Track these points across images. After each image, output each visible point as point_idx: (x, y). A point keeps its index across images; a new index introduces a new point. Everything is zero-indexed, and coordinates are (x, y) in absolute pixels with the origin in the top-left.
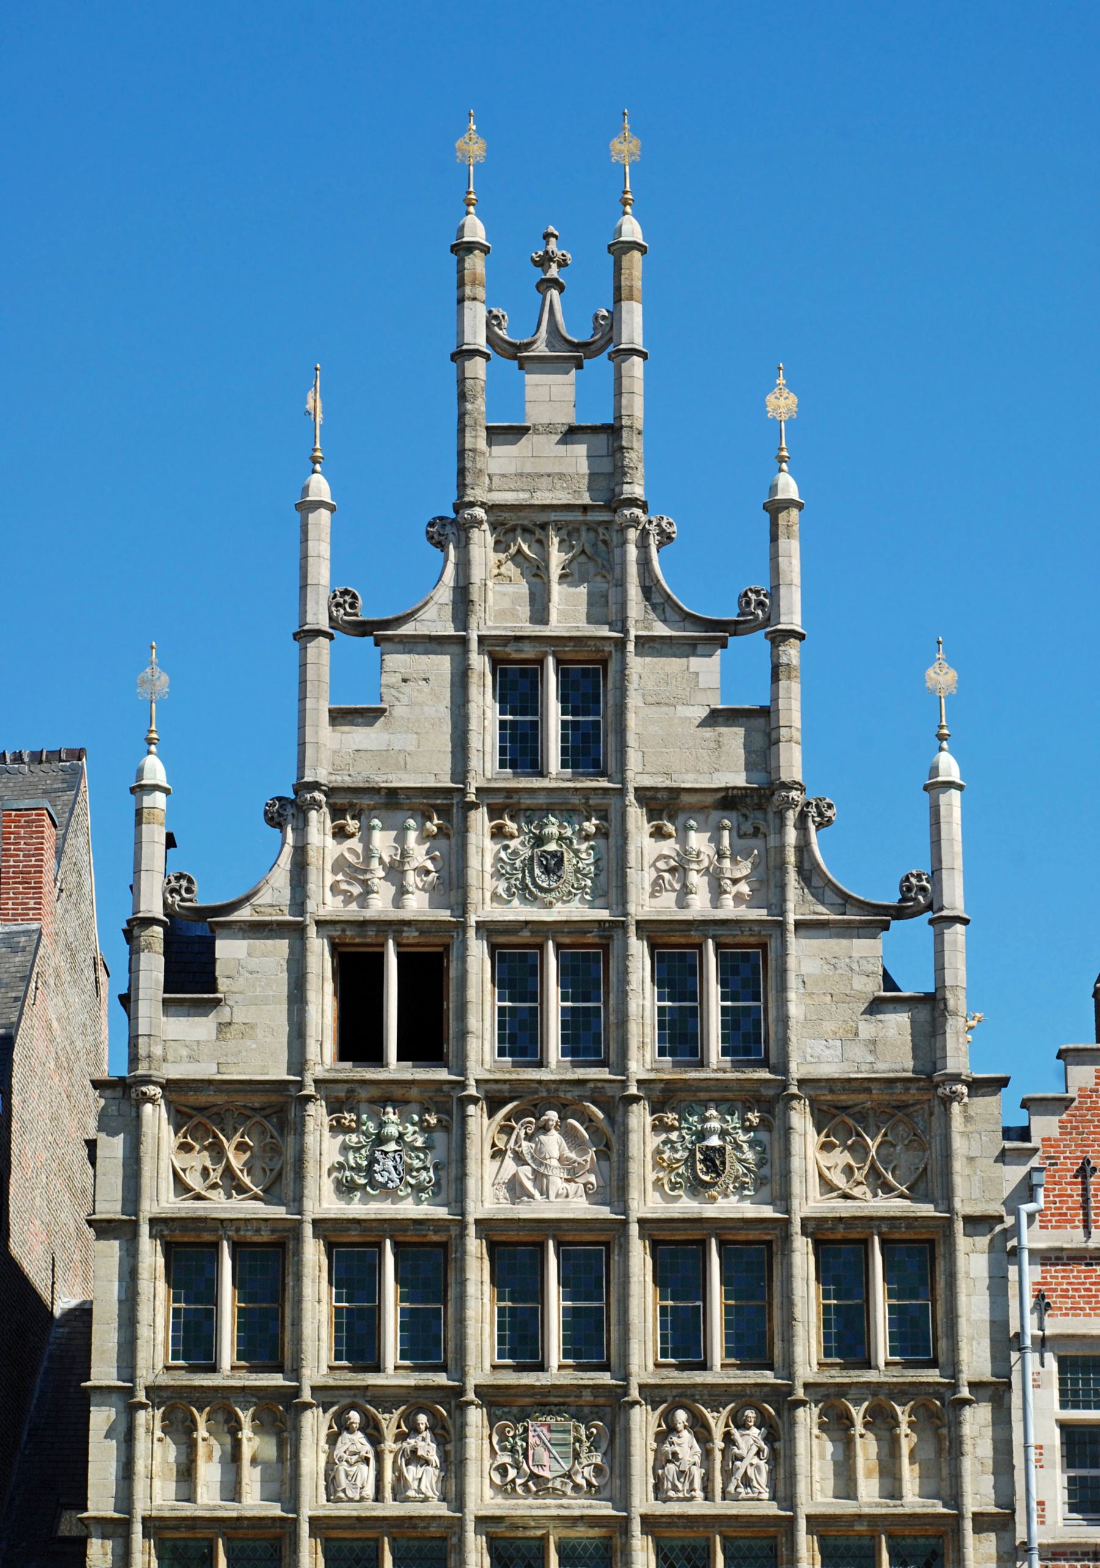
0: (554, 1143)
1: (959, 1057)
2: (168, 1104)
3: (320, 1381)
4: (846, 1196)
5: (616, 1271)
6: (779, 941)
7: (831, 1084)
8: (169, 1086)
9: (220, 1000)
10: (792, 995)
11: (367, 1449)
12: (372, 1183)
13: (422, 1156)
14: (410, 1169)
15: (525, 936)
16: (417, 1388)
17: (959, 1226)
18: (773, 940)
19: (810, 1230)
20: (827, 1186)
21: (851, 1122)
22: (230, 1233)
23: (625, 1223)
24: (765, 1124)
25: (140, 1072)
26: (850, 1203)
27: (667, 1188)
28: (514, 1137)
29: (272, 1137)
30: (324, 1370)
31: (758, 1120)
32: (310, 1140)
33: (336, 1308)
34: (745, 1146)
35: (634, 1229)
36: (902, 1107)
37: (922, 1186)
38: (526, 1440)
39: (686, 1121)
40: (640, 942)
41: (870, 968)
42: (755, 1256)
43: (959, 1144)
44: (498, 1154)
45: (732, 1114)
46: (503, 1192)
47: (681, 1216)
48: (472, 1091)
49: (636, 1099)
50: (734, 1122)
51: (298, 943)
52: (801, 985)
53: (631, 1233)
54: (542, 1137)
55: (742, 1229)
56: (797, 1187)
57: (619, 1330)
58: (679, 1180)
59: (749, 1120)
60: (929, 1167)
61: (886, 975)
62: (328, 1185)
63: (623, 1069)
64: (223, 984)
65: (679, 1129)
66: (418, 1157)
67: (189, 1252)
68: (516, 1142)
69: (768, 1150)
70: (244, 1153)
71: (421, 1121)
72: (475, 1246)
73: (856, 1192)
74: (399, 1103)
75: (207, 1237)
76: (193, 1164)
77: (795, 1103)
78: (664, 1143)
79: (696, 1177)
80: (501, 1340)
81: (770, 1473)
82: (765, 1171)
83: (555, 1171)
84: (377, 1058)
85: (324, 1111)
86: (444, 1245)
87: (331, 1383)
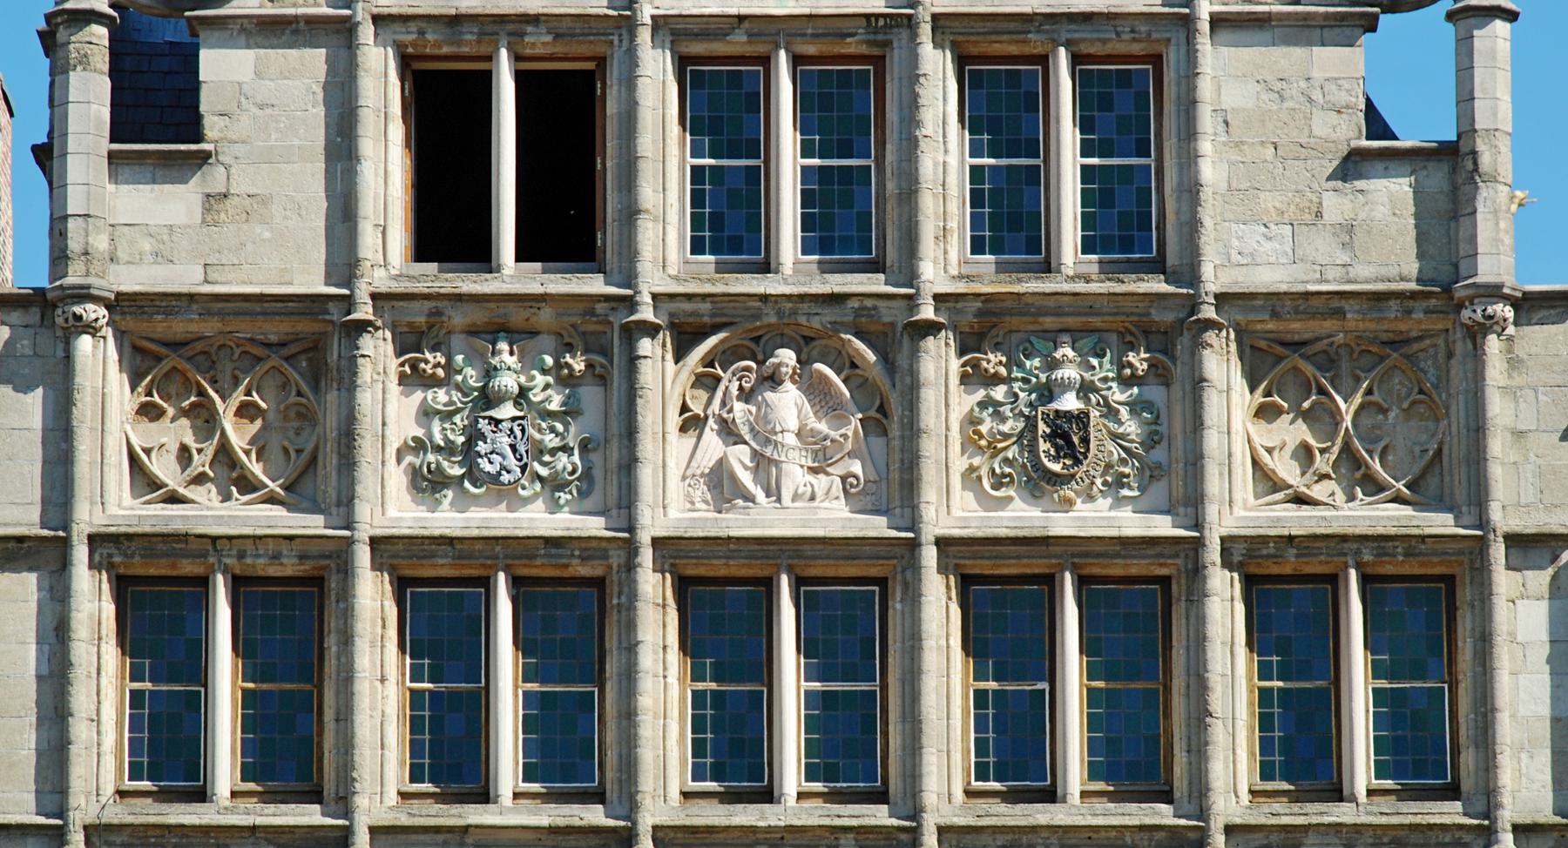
0: (789, 405)
1: (1498, 257)
2: (120, 336)
3: (386, 819)
4: (1300, 500)
5: (899, 628)
6: (1183, 50)
7: (1273, 301)
8: (120, 304)
9: (204, 157)
10: (1205, 146)
12: (473, 474)
13: (560, 427)
14: (539, 451)
15: (738, 43)
16: (553, 830)
17: (1498, 551)
18: (1172, 49)
19: (1236, 558)
20: (1267, 481)
21: (1309, 369)
22: (228, 561)
23: (914, 545)
24: (1159, 373)
25: (70, 280)
26: (1306, 511)
27: (986, 484)
28: (719, 394)
29: (299, 394)
30: (392, 798)
31: (1145, 366)
32: (366, 399)
33: (412, 691)
34: (1124, 412)
35: (930, 555)
36: (1398, 342)
37: (1432, 482)
39: (1021, 366)
40: (939, 52)
41: (1342, 98)
42: (1140, 604)
43: (1498, 408)
44: (692, 424)
45: (1101, 356)
46: (701, 491)
47: (1012, 533)
48: (646, 313)
49: (932, 328)
50: (1104, 368)
51: (343, 53)
52: (1221, 128)
53: (924, 563)
54: (769, 395)
55: (1118, 556)
56: (1214, 484)
58: (1008, 470)
59: (1130, 365)
60: (1445, 451)
61: (1371, 110)
62: (397, 478)
63: (910, 276)
64: (212, 126)
65: (1008, 380)
66: (552, 430)
67: (158, 592)
68: (723, 404)
69: (1164, 419)
70: (252, 421)
71: (559, 366)
72: (652, 585)
73: (1319, 491)
74: (519, 335)
75: (188, 568)
76: (163, 440)
77: (1210, 336)
78: (982, 405)
79: (1038, 466)
80: (698, 748)
82: (1159, 454)
83: (791, 454)
84: (480, 254)
85: (390, 348)
86: (599, 583)
87: (405, 820)
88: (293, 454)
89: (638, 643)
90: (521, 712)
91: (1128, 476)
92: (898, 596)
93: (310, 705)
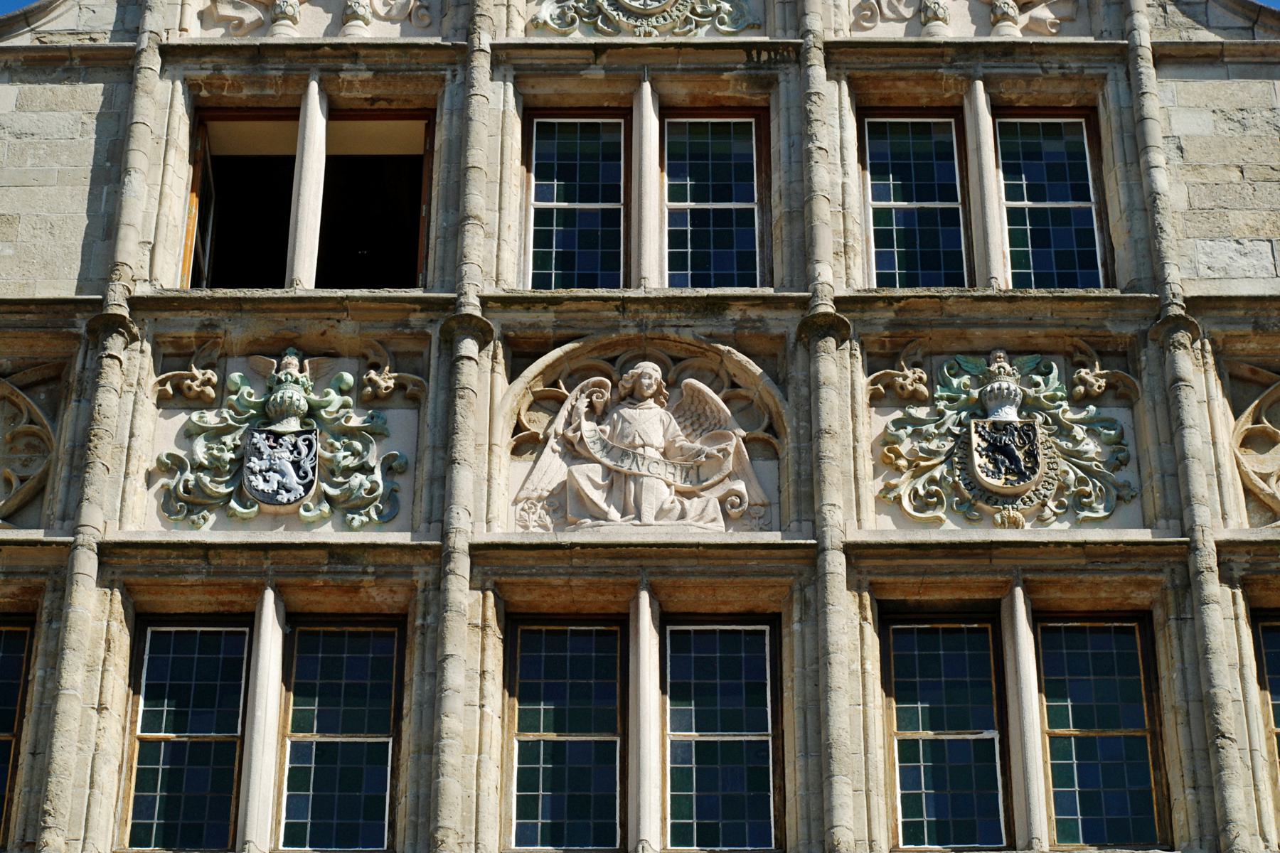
5: (797, 651)
6: (1123, 85)
10: (1157, 157)
13: (358, 445)
14: (330, 471)
18: (1110, 89)
19: (1237, 573)
23: (815, 554)
24: (1119, 393)
28: (564, 413)
29: (31, 422)
31: (1103, 382)
33: (141, 740)
34: (1079, 432)
35: (836, 564)
39: (946, 385)
40: (833, 86)
44: (526, 444)
45: (1046, 373)
50: (1052, 384)
51: (123, 88)
52: (1175, 154)
53: (829, 568)
54: (626, 412)
55: (1083, 571)
57: (806, 769)
58: (934, 488)
59: (1083, 381)
65: (930, 401)
66: (347, 448)
68: (568, 423)
69: (1129, 438)
71: (360, 385)
72: (468, 607)
78: (899, 424)
79: (972, 482)
80: (526, 807)
85: (148, 361)
86: (399, 620)
88: (15, 483)
89: (446, 657)
90: (287, 765)
91: (1089, 495)
92: (796, 615)
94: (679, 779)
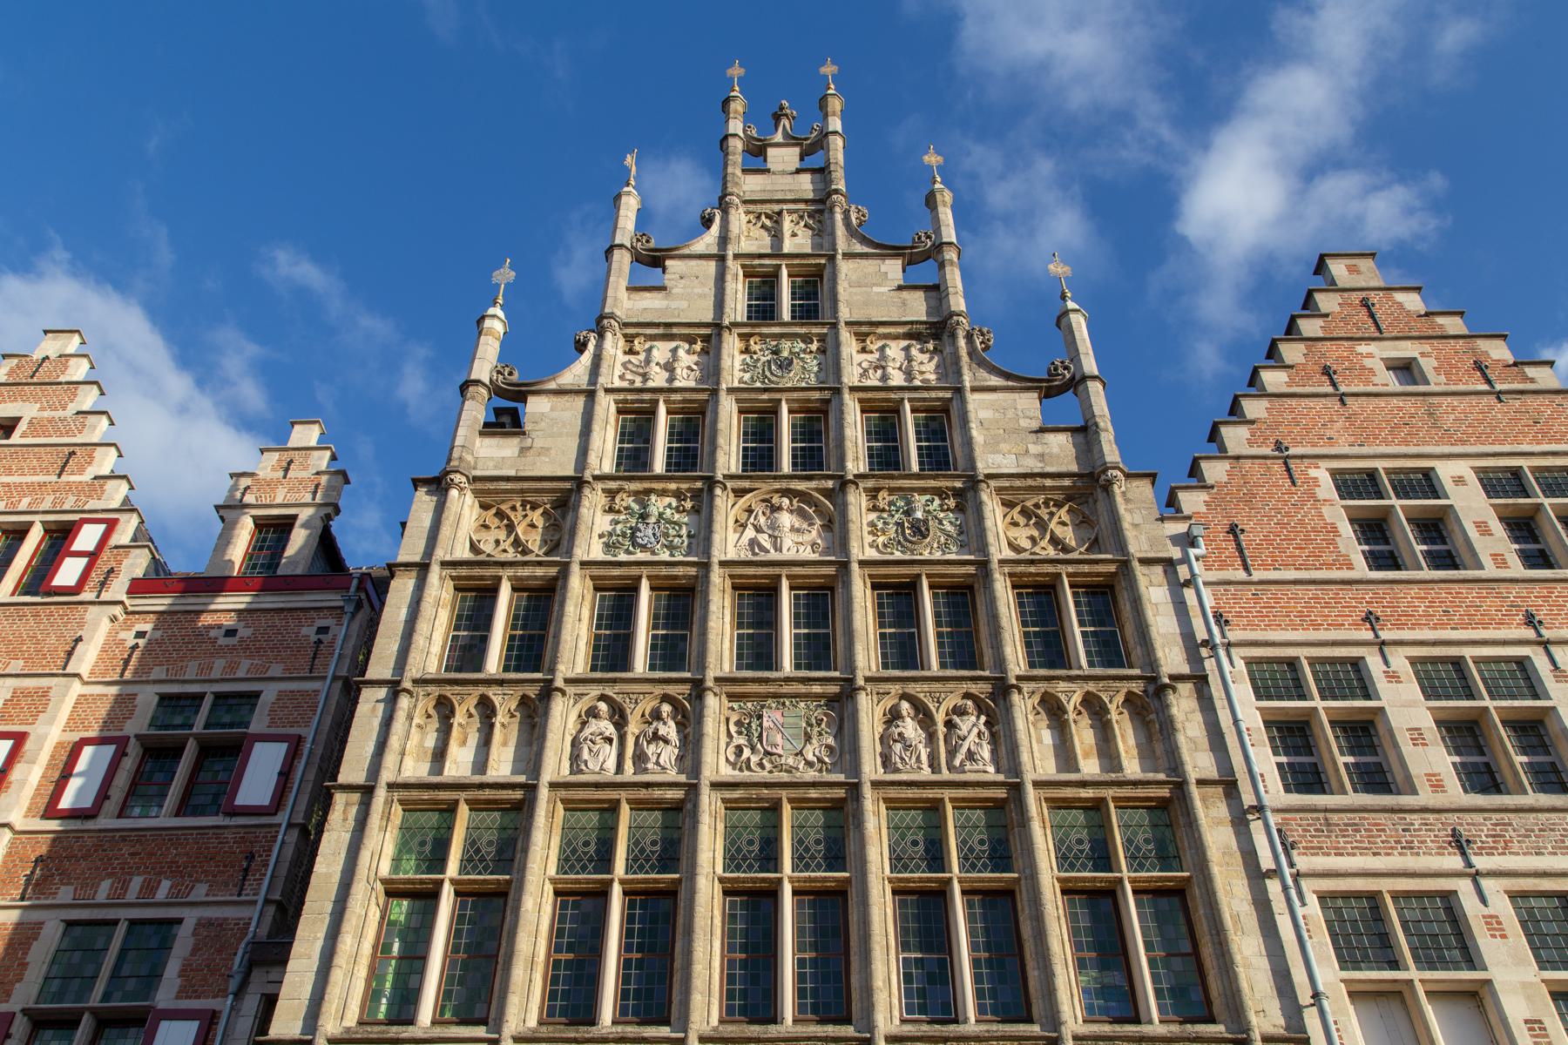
10: (973, 425)
11: (610, 730)
35: (855, 567)
38: (761, 725)
80: (740, 656)
81: (994, 752)
93: (542, 639)
94: (797, 646)
